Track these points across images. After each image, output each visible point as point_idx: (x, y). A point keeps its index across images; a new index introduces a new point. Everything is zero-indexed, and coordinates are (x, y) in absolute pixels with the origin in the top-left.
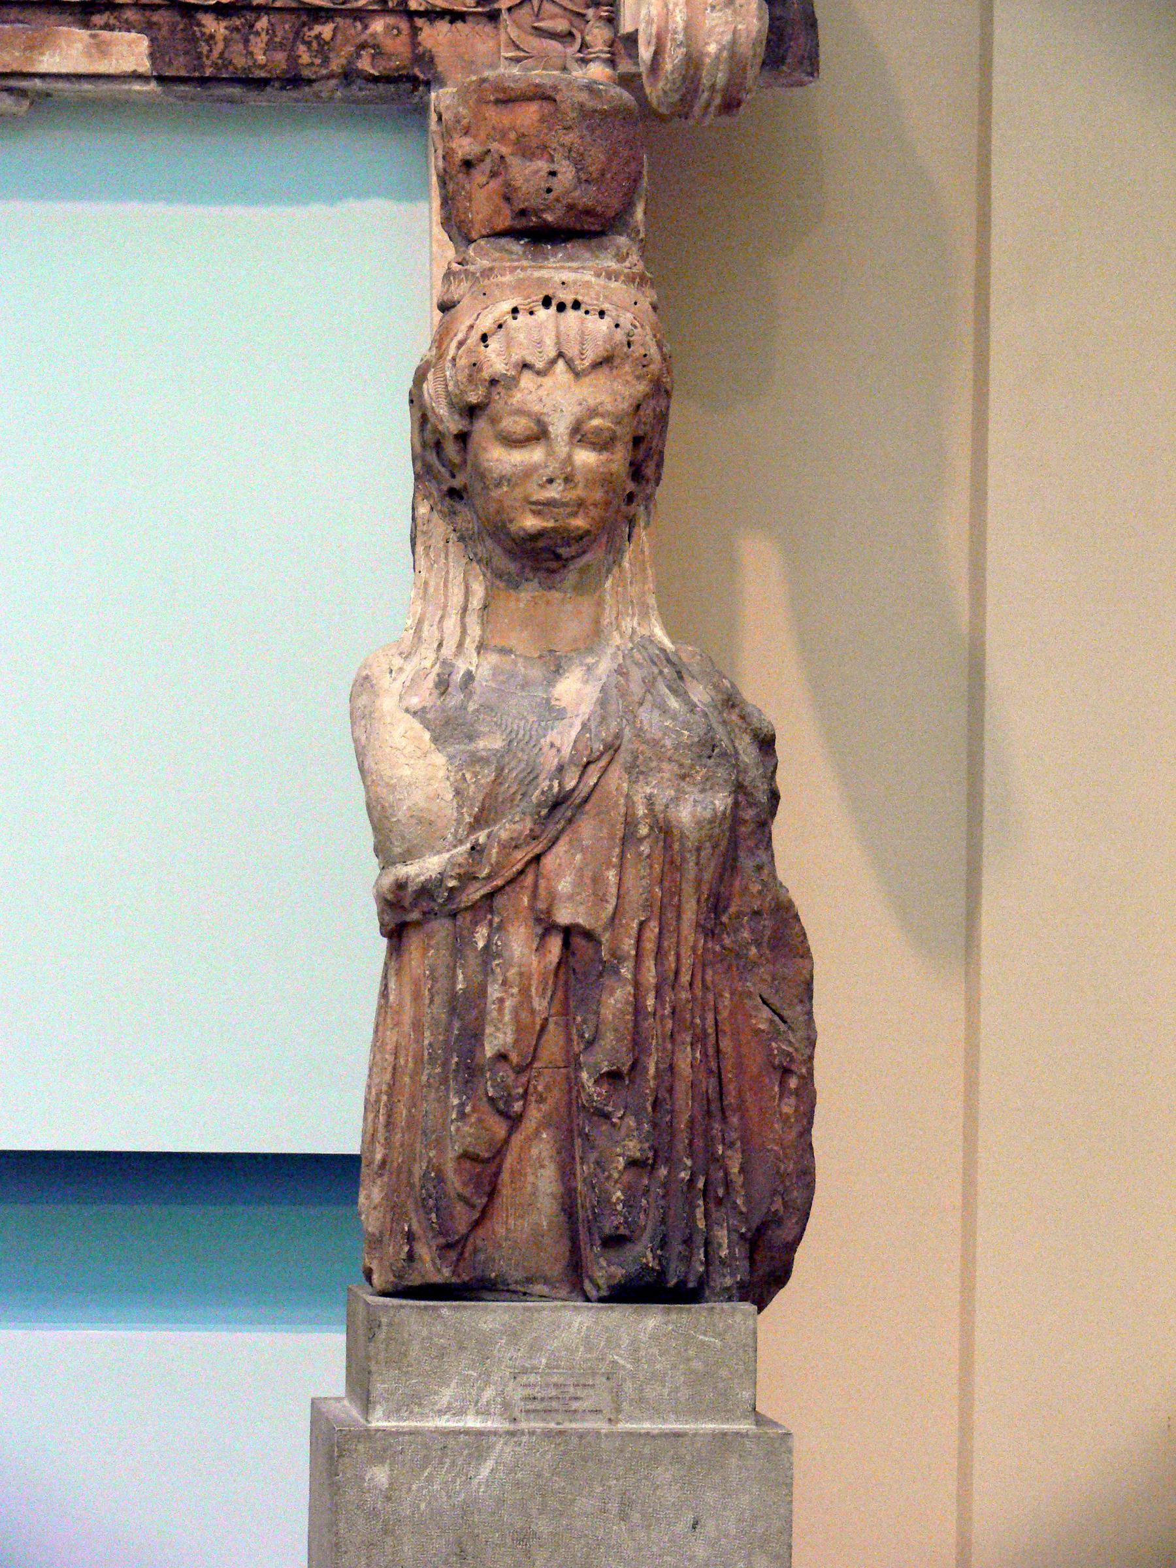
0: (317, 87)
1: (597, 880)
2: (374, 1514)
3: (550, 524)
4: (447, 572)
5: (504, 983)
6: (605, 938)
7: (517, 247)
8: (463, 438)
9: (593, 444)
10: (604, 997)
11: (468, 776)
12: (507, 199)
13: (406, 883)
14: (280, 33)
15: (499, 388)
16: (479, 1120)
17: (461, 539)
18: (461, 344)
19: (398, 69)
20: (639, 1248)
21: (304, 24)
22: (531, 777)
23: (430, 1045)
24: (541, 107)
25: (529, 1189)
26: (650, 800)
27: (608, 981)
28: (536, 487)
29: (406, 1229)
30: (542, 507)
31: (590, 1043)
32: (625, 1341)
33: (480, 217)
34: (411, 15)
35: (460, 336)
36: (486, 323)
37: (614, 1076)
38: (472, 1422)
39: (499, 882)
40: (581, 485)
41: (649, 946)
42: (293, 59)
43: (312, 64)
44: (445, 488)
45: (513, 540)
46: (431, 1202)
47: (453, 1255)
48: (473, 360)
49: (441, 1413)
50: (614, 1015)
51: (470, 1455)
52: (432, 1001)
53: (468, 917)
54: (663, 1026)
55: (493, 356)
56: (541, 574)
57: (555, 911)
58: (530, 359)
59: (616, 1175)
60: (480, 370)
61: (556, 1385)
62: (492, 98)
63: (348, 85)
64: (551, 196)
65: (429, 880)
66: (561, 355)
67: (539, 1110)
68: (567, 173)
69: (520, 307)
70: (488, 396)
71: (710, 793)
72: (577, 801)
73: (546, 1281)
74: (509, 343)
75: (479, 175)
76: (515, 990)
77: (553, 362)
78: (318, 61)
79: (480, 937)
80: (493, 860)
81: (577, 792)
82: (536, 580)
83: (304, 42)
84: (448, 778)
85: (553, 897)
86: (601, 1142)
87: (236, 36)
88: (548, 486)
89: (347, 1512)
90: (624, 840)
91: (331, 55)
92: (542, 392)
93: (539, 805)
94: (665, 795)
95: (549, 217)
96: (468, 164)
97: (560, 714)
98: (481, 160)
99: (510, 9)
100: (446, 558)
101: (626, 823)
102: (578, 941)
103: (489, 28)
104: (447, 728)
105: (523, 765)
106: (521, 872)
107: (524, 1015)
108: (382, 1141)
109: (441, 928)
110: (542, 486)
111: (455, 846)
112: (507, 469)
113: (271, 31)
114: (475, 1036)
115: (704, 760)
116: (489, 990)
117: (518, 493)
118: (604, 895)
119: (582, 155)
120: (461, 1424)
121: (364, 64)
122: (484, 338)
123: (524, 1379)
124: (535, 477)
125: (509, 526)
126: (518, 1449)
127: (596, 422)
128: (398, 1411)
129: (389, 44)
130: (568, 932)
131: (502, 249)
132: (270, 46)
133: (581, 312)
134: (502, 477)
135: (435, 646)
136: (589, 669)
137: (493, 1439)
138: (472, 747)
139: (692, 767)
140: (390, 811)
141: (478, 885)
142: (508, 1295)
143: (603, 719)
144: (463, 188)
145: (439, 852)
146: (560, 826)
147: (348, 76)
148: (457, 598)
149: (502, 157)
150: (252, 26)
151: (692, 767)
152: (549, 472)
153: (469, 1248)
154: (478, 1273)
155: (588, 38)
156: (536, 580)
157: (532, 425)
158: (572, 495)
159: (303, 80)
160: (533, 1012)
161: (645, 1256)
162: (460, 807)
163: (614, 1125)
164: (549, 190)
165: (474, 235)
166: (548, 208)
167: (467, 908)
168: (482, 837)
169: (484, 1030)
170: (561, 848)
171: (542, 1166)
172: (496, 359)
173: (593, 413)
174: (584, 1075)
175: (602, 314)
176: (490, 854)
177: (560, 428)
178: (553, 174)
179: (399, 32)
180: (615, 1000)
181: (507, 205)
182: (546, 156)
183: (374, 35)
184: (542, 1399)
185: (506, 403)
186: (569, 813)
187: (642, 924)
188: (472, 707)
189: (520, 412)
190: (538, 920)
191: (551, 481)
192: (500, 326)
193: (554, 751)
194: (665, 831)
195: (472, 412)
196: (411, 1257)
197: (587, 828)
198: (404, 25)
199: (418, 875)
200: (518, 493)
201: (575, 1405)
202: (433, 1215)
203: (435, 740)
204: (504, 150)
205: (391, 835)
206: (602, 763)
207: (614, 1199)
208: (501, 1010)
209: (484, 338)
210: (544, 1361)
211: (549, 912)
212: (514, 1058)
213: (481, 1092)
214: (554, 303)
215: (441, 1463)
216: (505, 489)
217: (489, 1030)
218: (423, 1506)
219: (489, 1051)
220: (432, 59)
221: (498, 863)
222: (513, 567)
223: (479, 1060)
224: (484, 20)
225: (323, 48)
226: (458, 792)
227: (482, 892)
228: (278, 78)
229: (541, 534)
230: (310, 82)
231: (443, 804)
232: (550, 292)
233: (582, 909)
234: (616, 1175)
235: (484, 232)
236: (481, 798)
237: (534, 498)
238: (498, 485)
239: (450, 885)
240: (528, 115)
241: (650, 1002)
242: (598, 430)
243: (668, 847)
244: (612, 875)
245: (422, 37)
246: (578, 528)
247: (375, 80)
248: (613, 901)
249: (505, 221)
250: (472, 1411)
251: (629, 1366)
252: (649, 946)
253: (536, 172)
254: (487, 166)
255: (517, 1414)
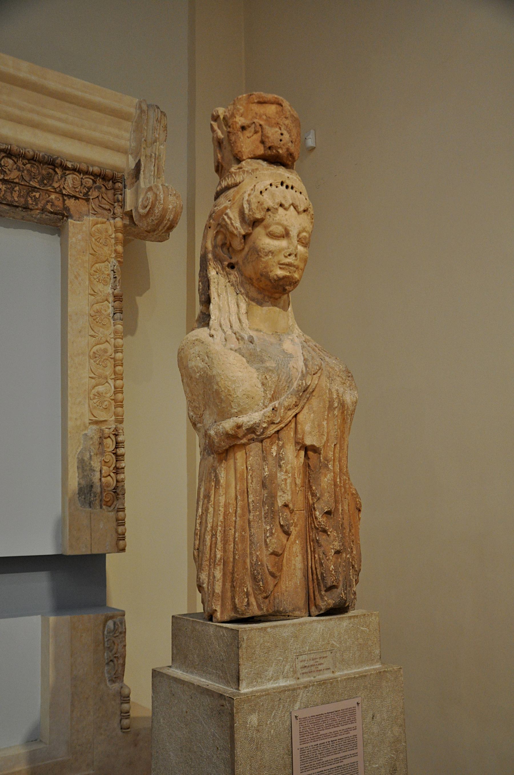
0: (32, 212)
1: (320, 425)
2: (252, 740)
3: (288, 274)
4: (228, 299)
5: (286, 472)
6: (322, 452)
7: (265, 164)
8: (245, 237)
9: (303, 243)
10: (322, 478)
11: (268, 377)
12: (263, 142)
13: (242, 425)
14: (22, 192)
15: (270, 213)
16: (278, 536)
17: (232, 285)
18: (249, 195)
19: (59, 210)
20: (339, 590)
21: (30, 191)
22: (289, 381)
23: (253, 501)
24: (276, 108)
25: (293, 567)
26: (337, 390)
27: (323, 471)
28: (283, 257)
29: (246, 590)
30: (283, 266)
31: (319, 499)
32: (336, 634)
33: (247, 150)
34: (63, 195)
35: (248, 192)
36: (260, 187)
37: (329, 513)
38: (282, 683)
39: (282, 425)
40: (298, 260)
41: (337, 455)
42: (26, 201)
43: (32, 204)
44: (226, 263)
45: (270, 280)
46: (260, 577)
47: (267, 601)
48: (259, 200)
49: (269, 680)
50: (327, 486)
51: (290, 701)
52: (252, 481)
53: (268, 440)
54: (341, 490)
55: (267, 199)
56: (271, 299)
57: (305, 439)
58: (283, 202)
59: (331, 558)
60: (262, 204)
61: (313, 660)
62: (256, 101)
63: (43, 213)
64: (282, 143)
65: (255, 424)
66: (292, 204)
67: (295, 530)
68: (286, 136)
69: (273, 184)
70: (265, 216)
71: (352, 391)
72: (311, 390)
73: (299, 610)
74: (273, 195)
75: (248, 133)
76: (290, 475)
77: (290, 206)
78: (34, 203)
79: (274, 450)
80: (282, 415)
81: (310, 387)
82: (270, 302)
83: (30, 197)
84: (258, 378)
85: (304, 433)
86: (322, 543)
87: (8, 190)
88: (289, 257)
89: (241, 742)
90: (329, 408)
91: (39, 202)
92: (287, 217)
93: (298, 391)
94: (341, 390)
95: (280, 151)
96: (243, 128)
97: (291, 356)
98: (249, 127)
99: (92, 199)
100: (226, 292)
101: (329, 402)
102: (310, 453)
103: (86, 204)
104: (254, 358)
105: (285, 375)
106: (290, 421)
107: (293, 486)
108: (220, 549)
109: (255, 448)
110: (286, 257)
111: (264, 409)
112: (272, 248)
113: (20, 192)
114: (273, 497)
115: (348, 378)
116: (278, 475)
117: (276, 259)
118: (323, 432)
119: (290, 130)
120: (277, 685)
121: (49, 207)
122: (261, 192)
123: (301, 658)
124: (283, 252)
125: (270, 273)
126: (308, 694)
127: (304, 234)
128: (252, 682)
129: (56, 203)
130: (306, 449)
131: (258, 164)
132: (19, 196)
133: (293, 191)
134: (270, 251)
135: (229, 327)
136: (292, 340)
137: (299, 691)
138: (264, 365)
139: (346, 379)
140: (233, 392)
141: (274, 426)
142: (282, 618)
143: (313, 358)
144: (240, 138)
145: (256, 411)
146: (305, 401)
147: (43, 210)
148: (233, 308)
149: (260, 125)
150: (13, 189)
151: (346, 379)
152: (290, 251)
153: (272, 597)
154: (276, 609)
155: (115, 211)
156: (270, 302)
157: (283, 230)
158: (296, 263)
159: (28, 208)
160: (296, 484)
161: (342, 594)
162: (265, 391)
163: (328, 535)
164: (281, 140)
165: (244, 158)
166: (280, 148)
167: (269, 437)
168: (276, 403)
169: (277, 493)
170: (305, 411)
171: (297, 556)
172: (268, 201)
173: (304, 230)
174: (317, 513)
175: (301, 193)
176: (280, 413)
177: (294, 233)
178: (282, 134)
179: (59, 200)
180: (326, 480)
181: (262, 145)
182: (278, 127)
183: (52, 199)
184: (309, 666)
185: (273, 219)
186: (308, 396)
187: (335, 445)
188: (258, 350)
189: (279, 224)
190: (297, 443)
191: (290, 255)
192: (266, 190)
193: (295, 370)
194: (342, 404)
195: (255, 223)
196: (248, 604)
197: (315, 402)
198: (61, 198)
199: (249, 422)
200: (276, 259)
201: (320, 667)
202: (261, 583)
203: (248, 362)
204: (262, 123)
205: (232, 404)
206: (318, 374)
207: (331, 569)
208: (286, 484)
209: (261, 192)
210: (307, 648)
211: (303, 439)
212: (291, 505)
213: (278, 523)
214: (285, 185)
215: (279, 707)
216: (270, 257)
217: (279, 494)
218: (272, 731)
219: (280, 504)
220: (69, 209)
221: (283, 416)
222: (260, 297)
223: (276, 508)
224: (84, 201)
225: (36, 200)
226: (263, 384)
227: (276, 430)
228: (21, 207)
229: (285, 277)
230: (31, 210)
231: (258, 389)
232: (284, 180)
233: (315, 438)
234: (331, 558)
235: (250, 156)
236: (274, 387)
237: (282, 262)
238: (266, 255)
239: (264, 426)
240: (272, 109)
241: (338, 480)
242: (305, 238)
243: (343, 413)
244: (325, 423)
245: (66, 202)
246: (296, 278)
247: (51, 213)
248: (326, 435)
249: (261, 151)
250: (281, 677)
251: (338, 645)
252: (337, 455)
253: (276, 132)
254: (252, 129)
255: (299, 676)
